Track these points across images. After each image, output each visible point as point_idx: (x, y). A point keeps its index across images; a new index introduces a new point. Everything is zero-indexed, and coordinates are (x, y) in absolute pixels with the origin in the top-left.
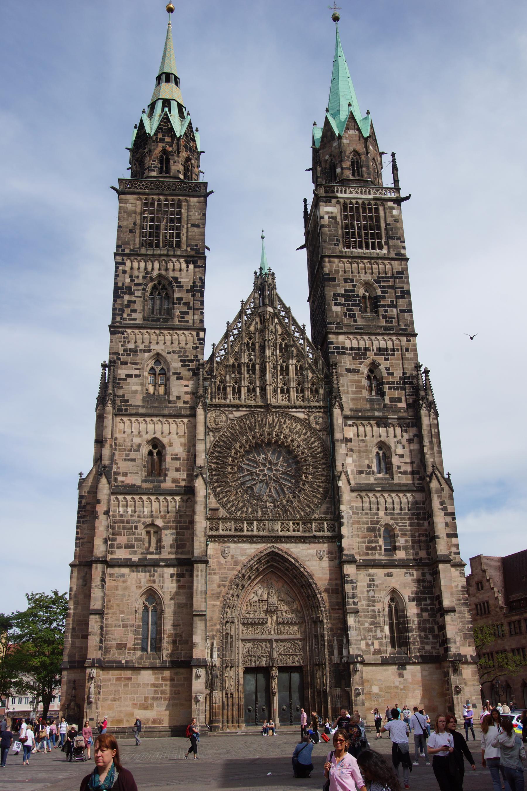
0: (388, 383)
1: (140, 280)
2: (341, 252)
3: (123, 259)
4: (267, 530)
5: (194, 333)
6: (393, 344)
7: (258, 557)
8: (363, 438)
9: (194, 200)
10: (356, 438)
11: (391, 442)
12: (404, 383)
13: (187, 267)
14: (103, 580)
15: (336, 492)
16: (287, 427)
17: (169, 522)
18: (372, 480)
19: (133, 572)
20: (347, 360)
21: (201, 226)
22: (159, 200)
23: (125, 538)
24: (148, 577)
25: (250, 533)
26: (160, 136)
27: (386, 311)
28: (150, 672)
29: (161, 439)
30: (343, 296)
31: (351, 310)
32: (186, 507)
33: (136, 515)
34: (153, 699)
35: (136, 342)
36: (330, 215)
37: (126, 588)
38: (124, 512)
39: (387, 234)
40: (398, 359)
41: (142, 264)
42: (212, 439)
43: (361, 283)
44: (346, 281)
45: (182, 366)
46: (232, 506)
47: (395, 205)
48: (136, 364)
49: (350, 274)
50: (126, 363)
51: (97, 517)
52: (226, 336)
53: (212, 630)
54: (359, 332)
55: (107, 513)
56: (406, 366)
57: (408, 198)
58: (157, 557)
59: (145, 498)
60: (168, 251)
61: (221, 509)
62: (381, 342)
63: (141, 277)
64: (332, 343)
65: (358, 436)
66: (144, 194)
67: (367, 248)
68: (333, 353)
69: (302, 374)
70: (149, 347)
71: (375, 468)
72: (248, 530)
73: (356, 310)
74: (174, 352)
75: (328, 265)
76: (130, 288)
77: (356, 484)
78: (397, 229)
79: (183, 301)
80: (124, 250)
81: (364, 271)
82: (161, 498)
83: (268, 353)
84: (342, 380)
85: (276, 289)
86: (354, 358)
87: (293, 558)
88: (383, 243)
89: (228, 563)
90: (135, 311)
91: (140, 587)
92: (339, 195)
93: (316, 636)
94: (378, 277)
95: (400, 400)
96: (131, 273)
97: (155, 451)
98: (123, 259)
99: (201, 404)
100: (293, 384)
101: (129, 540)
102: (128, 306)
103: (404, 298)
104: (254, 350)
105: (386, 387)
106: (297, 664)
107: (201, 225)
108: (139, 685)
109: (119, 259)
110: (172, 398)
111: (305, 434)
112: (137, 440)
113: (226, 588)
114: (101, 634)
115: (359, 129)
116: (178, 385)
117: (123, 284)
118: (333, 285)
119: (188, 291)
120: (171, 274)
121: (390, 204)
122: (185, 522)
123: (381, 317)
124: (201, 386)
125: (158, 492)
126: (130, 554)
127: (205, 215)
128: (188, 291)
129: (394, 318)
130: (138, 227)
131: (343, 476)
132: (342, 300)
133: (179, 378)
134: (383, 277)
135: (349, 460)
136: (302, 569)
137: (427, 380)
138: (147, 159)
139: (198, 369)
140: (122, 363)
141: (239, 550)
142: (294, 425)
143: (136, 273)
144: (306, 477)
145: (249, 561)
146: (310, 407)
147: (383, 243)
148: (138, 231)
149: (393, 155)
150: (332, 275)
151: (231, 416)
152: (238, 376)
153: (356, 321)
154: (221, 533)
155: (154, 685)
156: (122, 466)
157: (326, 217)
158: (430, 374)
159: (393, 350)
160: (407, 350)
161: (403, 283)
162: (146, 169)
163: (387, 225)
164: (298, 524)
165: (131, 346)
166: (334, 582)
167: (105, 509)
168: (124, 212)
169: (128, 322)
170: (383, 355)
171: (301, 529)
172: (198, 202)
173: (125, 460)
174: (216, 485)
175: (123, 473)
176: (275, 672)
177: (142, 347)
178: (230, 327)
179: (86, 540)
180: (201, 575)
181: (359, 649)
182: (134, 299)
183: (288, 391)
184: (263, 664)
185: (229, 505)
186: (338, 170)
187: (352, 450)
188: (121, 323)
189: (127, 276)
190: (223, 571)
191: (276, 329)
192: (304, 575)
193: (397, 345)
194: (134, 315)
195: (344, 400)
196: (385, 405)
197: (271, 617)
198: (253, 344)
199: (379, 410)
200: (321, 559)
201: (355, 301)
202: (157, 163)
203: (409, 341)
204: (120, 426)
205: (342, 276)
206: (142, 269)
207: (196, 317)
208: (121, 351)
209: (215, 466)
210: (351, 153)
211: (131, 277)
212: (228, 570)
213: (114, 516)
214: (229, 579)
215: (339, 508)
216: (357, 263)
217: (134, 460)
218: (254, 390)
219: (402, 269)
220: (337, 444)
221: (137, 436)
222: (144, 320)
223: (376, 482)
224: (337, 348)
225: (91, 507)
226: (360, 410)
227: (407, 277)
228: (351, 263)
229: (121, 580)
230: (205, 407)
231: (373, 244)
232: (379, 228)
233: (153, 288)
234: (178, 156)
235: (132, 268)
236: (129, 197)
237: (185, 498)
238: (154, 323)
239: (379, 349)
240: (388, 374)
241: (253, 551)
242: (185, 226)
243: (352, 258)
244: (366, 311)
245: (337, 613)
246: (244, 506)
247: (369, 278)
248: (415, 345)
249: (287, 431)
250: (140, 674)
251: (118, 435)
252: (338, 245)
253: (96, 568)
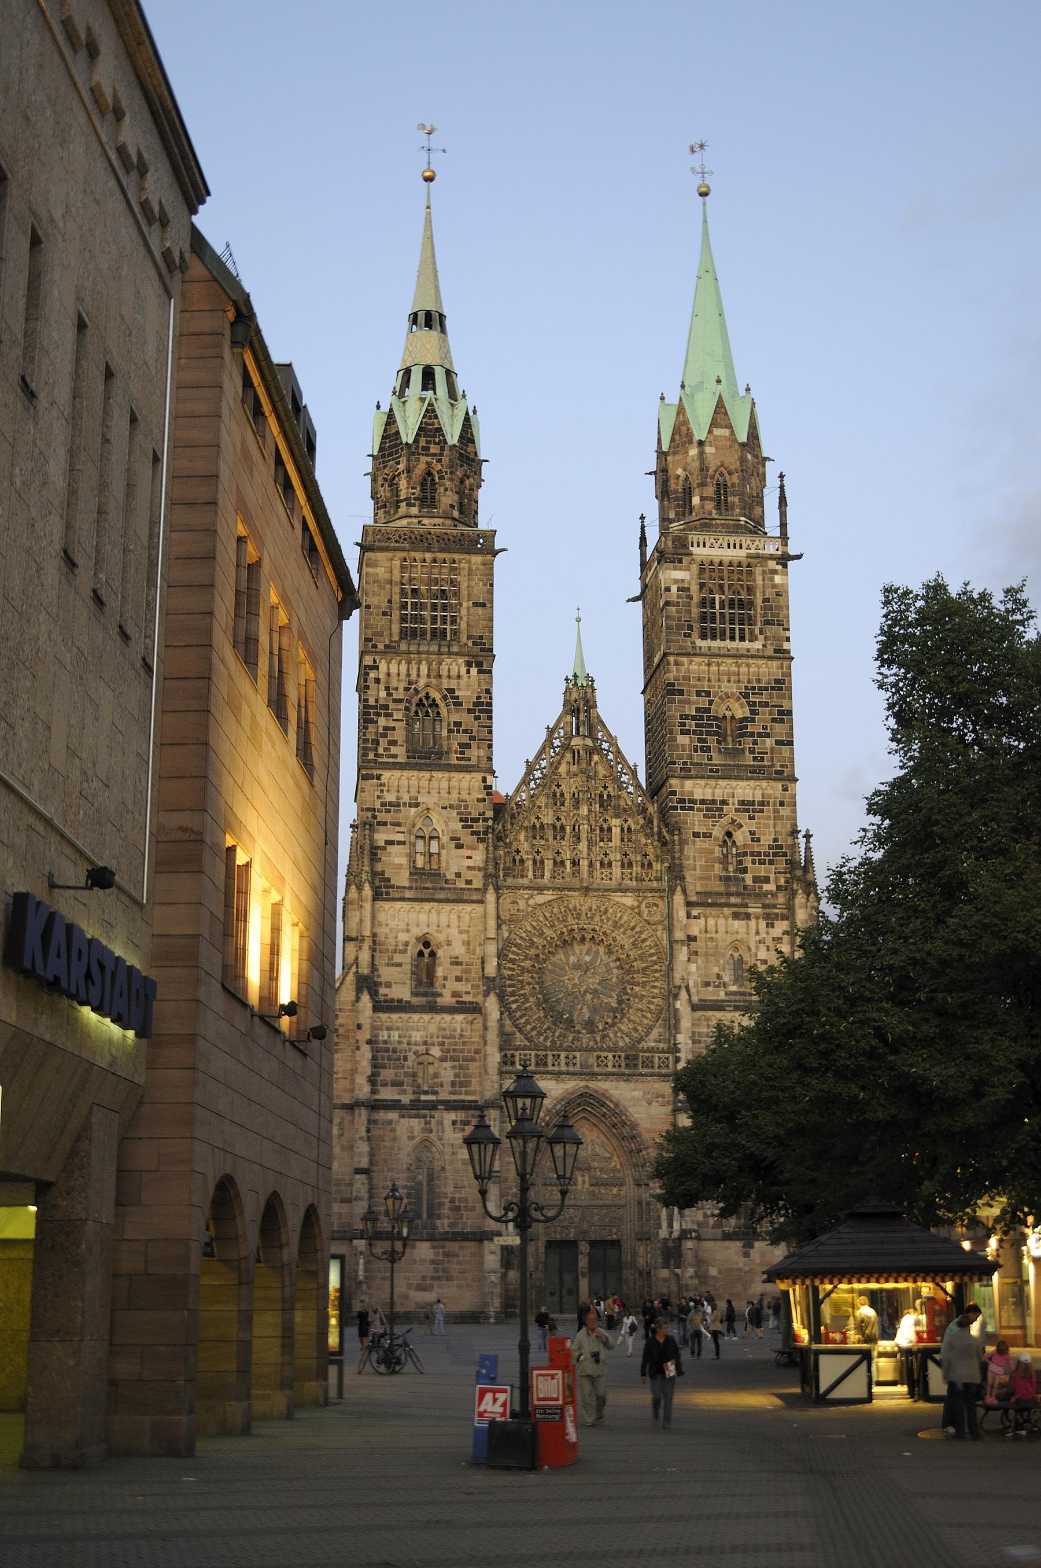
0: (752, 854)
1: (400, 694)
2: (694, 648)
3: (375, 661)
4: (578, 1065)
5: (478, 776)
6: (763, 796)
8: (713, 935)
9: (477, 559)
10: (704, 935)
11: (753, 939)
12: (775, 855)
13: (468, 672)
14: (368, 1131)
15: (672, 1012)
16: (608, 919)
17: (448, 1051)
18: (722, 995)
19: (403, 1117)
20: (696, 819)
21: (488, 605)
22: (424, 561)
23: (392, 1071)
24: (423, 1125)
25: (556, 1069)
26: (422, 442)
27: (755, 743)
28: (428, 1244)
29: (436, 935)
30: (694, 718)
31: (704, 741)
32: (472, 1031)
33: (405, 1040)
34: (433, 1278)
35: (398, 791)
36: (681, 585)
37: (394, 1139)
38: (389, 1037)
39: (765, 615)
40: (769, 818)
41: (403, 668)
42: (506, 935)
43: (720, 698)
44: (698, 694)
45: (463, 827)
46: (533, 1029)
47: (780, 567)
48: (399, 825)
49: (706, 683)
50: (385, 824)
51: (358, 1048)
52: (525, 782)
53: (507, 1194)
54: (716, 774)
55: (369, 1042)
56: (778, 829)
57: (799, 557)
58: (434, 1098)
59: (416, 1017)
60: (440, 646)
61: (518, 1035)
62: (746, 790)
63: (401, 690)
64: (674, 793)
65: (706, 932)
66: (403, 550)
67: (733, 638)
68: (676, 808)
69: (629, 840)
70: (417, 799)
71: (727, 978)
72: (553, 1065)
73: (712, 741)
74: (451, 807)
75: (674, 668)
76: (387, 707)
77: (700, 1000)
78: (779, 607)
79: (463, 728)
80: (375, 646)
81: (726, 677)
82: (438, 1017)
83: (584, 810)
84: (689, 851)
85: (596, 707)
86: (705, 816)
87: (612, 1101)
88: (757, 631)
90: (394, 743)
91: (412, 1138)
92: (695, 550)
93: (640, 1203)
94: (746, 688)
95: (767, 880)
96: (388, 682)
97: (427, 952)
98: (375, 661)
99: (491, 887)
100: (615, 857)
101: (396, 1075)
102: (385, 736)
103: (782, 721)
104: (563, 804)
105: (748, 861)
106: (615, 1237)
107: (485, 604)
108: (414, 1262)
109: (368, 660)
110: (450, 876)
111: (633, 929)
112: (403, 937)
114: (370, 1198)
115: (730, 426)
116: (458, 857)
117: (377, 701)
118: (680, 702)
119: (469, 711)
120: (445, 684)
121: (772, 564)
122: (469, 1051)
123: (747, 752)
124: (491, 860)
125: (432, 1008)
126: (399, 1094)
127: (492, 585)
128: (469, 711)
129: (766, 753)
130: (396, 605)
131: (683, 994)
132: (691, 725)
133: (459, 846)
134: (754, 688)
135: (693, 967)
137: (808, 848)
138: (403, 483)
139: (486, 833)
140: (379, 823)
142: (619, 915)
143: (394, 683)
144: (632, 989)
145: (556, 1105)
146: (639, 890)
147: (757, 631)
148: (396, 614)
149: (782, 476)
150: (679, 685)
151: (531, 902)
152: (543, 842)
153: (711, 759)
155: (433, 1262)
156: (386, 973)
157: (674, 589)
158: (811, 840)
159: (762, 804)
160: (782, 804)
161: (783, 697)
162: (402, 501)
163: (765, 600)
164: (619, 1057)
165: (391, 797)
167: (369, 1037)
168: (374, 582)
169: (385, 760)
170: (748, 811)
171: (623, 1065)
172: (484, 564)
173: (388, 965)
174: (512, 999)
175: (386, 983)
176: (584, 1248)
177: (406, 798)
178: (530, 767)
179: (340, 1075)
181: (693, 1222)
182: (392, 724)
183: (610, 864)
184: (571, 1237)
185: (529, 1027)
186: (696, 500)
187: (696, 953)
188: (375, 762)
189: (382, 686)
191: (596, 773)
193: (770, 796)
194: (394, 750)
195: (689, 879)
196: (745, 887)
197: (583, 1176)
198: (562, 795)
199: (737, 894)
201: (711, 726)
202: (417, 491)
203: (785, 789)
204: (381, 917)
205: (694, 686)
206: (403, 676)
207: (482, 753)
208: (378, 806)
209: (510, 973)
210: (715, 472)
211: (387, 688)
213: (376, 1042)
215: (675, 1037)
216: (718, 665)
217: (399, 965)
218: (562, 863)
219: (783, 674)
220: (676, 947)
221: (403, 931)
222: (408, 757)
223: (727, 998)
224: (682, 801)
225: (346, 1031)
226: (709, 894)
227: (789, 689)
228: (709, 665)
229: (389, 1128)
230: (497, 889)
231: (742, 630)
232: (751, 604)
233: (417, 705)
234: (451, 480)
235: (388, 674)
236: (380, 556)
237: (470, 1017)
238: (423, 761)
239: (742, 803)
240: (753, 840)
241: (560, 1092)
242: (465, 604)
243: (711, 654)
244: (725, 741)
246: (549, 1028)
247: (733, 688)
248: (794, 796)
249: (607, 927)
250: (414, 1247)
251: (378, 930)
252: (690, 636)
253: (360, 1115)
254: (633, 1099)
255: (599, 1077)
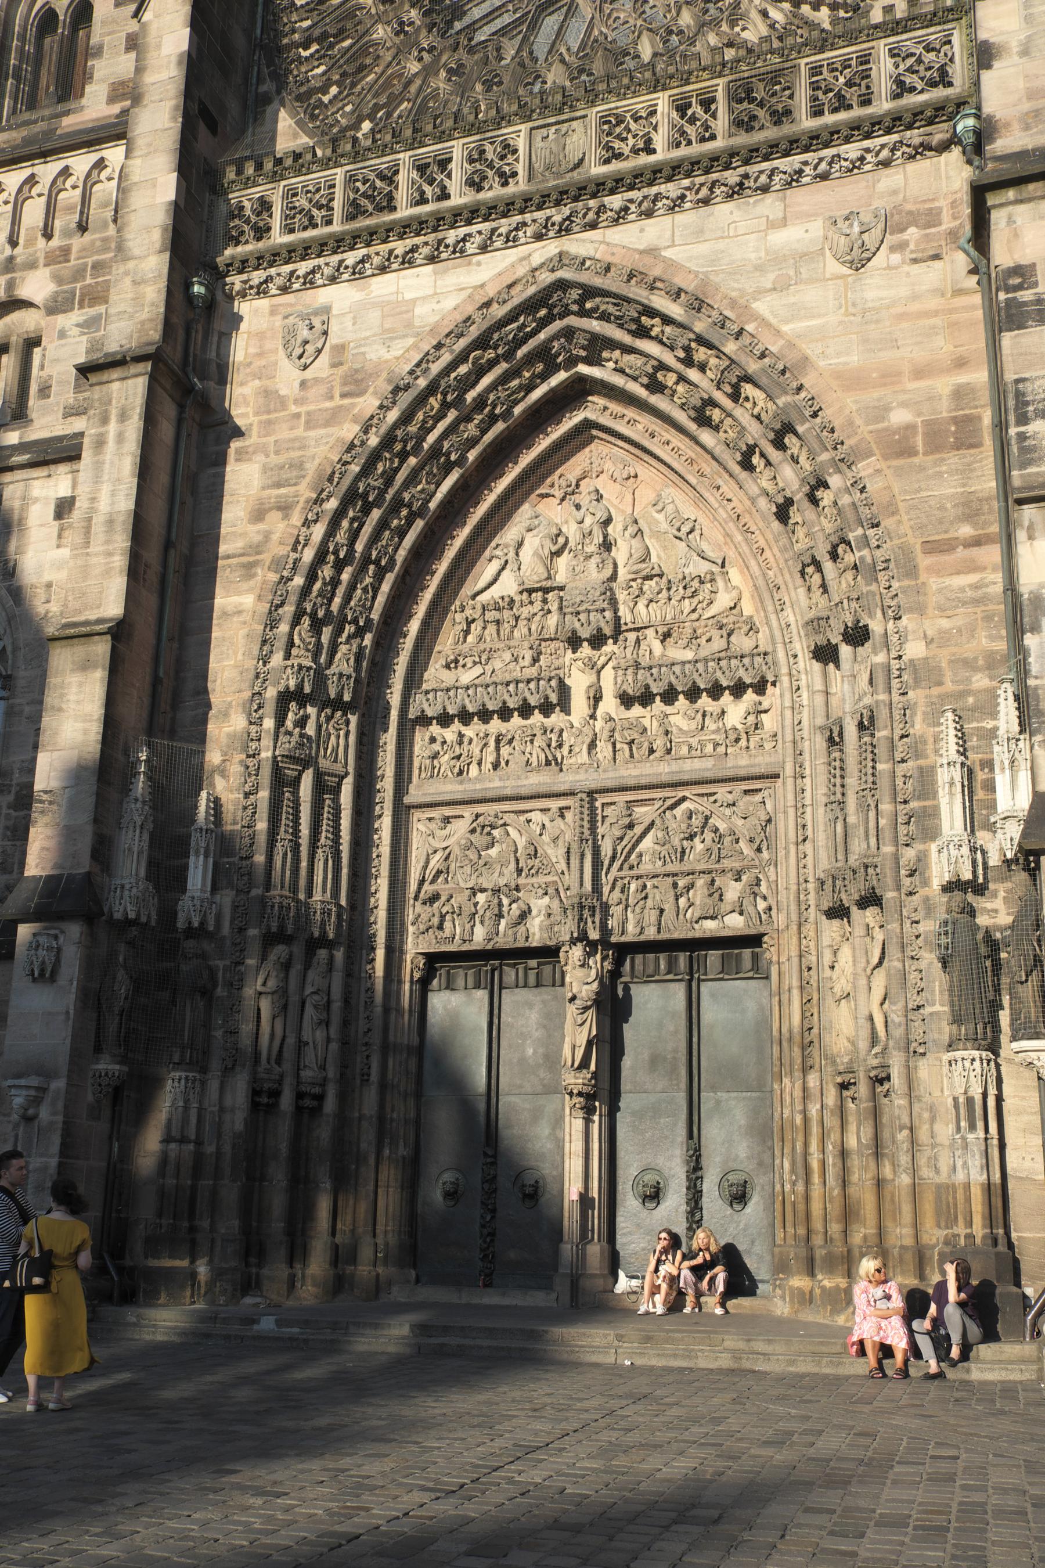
7: (474, 332)
89: (312, 393)
93: (835, 741)
106: (735, 924)
113: (297, 519)
136: (731, 348)
141: (374, 317)
154: (278, 238)
166: (944, 385)
180: (120, 438)
190: (283, 433)
192: (748, 379)
200: (859, 261)
212: (309, 425)
214: (311, 468)
241: (449, 303)
245: (973, 567)
254: (777, 259)
255: (615, 201)
